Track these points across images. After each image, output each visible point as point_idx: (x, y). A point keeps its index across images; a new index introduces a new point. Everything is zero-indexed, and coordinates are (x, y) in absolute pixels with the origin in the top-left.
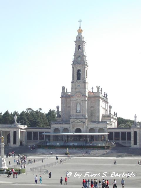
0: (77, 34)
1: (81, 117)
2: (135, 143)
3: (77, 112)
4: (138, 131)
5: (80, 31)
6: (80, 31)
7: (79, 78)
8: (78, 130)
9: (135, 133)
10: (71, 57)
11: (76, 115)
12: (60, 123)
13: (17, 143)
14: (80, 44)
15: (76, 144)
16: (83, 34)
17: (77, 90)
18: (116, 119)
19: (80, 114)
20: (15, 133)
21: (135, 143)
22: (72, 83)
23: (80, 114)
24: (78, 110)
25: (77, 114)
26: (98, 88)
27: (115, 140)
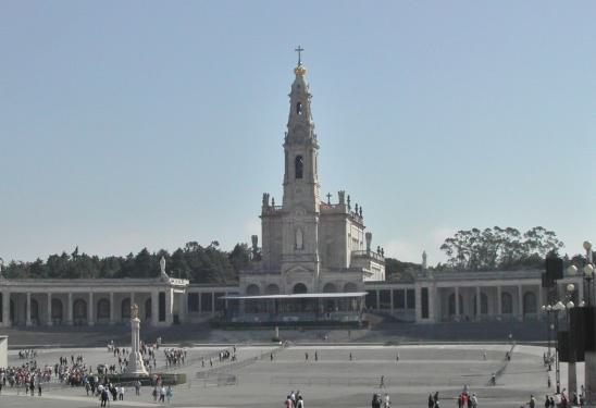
0: (293, 78)
1: (306, 258)
2: (425, 314)
3: (295, 248)
4: (430, 287)
5: (299, 73)
6: (299, 73)
7: (299, 175)
8: (301, 288)
9: (425, 292)
10: (281, 130)
12: (260, 274)
13: (167, 319)
14: (299, 99)
15: (295, 319)
16: (306, 79)
17: (297, 201)
18: (381, 263)
20: (162, 297)
21: (425, 314)
22: (285, 184)
24: (299, 243)
26: (341, 194)
27: (381, 307)
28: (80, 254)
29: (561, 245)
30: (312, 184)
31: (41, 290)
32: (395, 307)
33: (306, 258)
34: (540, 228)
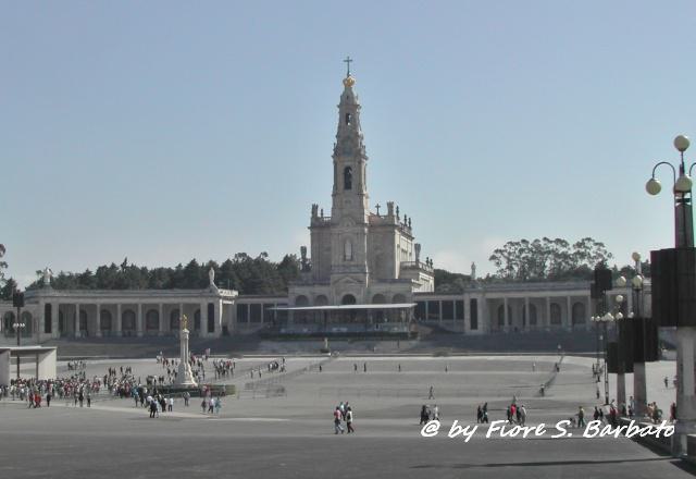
0: (342, 89)
1: (354, 269)
2: (474, 325)
3: (345, 259)
4: (479, 298)
5: (348, 84)
6: (348, 84)
7: (348, 186)
8: (350, 299)
9: (474, 303)
10: (331, 141)
11: (344, 266)
12: (308, 285)
13: (216, 330)
14: (348, 110)
15: (344, 330)
17: (345, 212)
18: (430, 274)
19: (352, 263)
20: (211, 308)
21: (474, 325)
22: (334, 195)
23: (352, 263)
24: (348, 254)
25: (346, 263)
26: (390, 205)
27: (430, 318)
28: (129, 264)
29: (610, 256)
30: (361, 195)
31: (90, 301)
32: (444, 318)
33: (354, 269)
34: (589, 239)
